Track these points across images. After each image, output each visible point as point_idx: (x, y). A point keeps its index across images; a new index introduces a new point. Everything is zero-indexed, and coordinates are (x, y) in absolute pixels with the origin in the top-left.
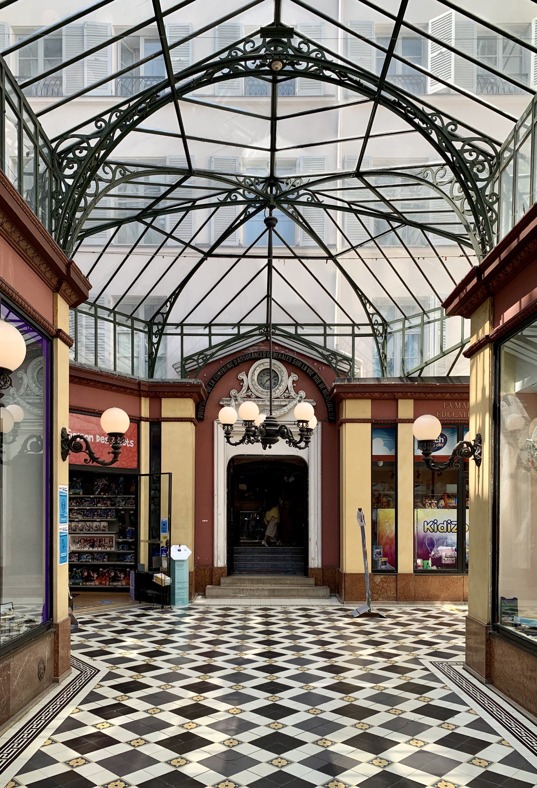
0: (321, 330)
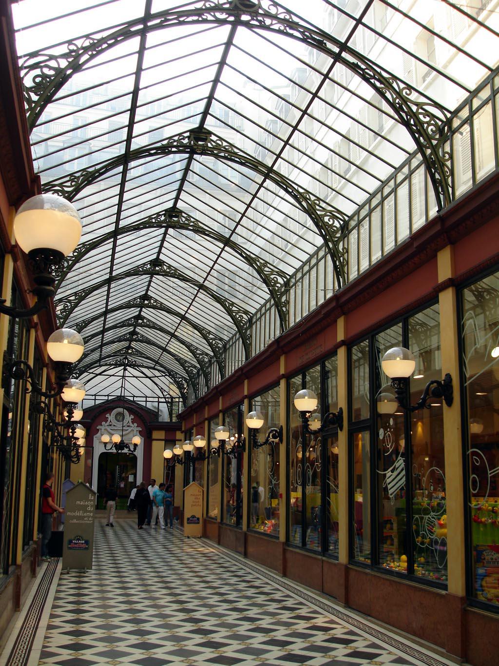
0: (144, 399)
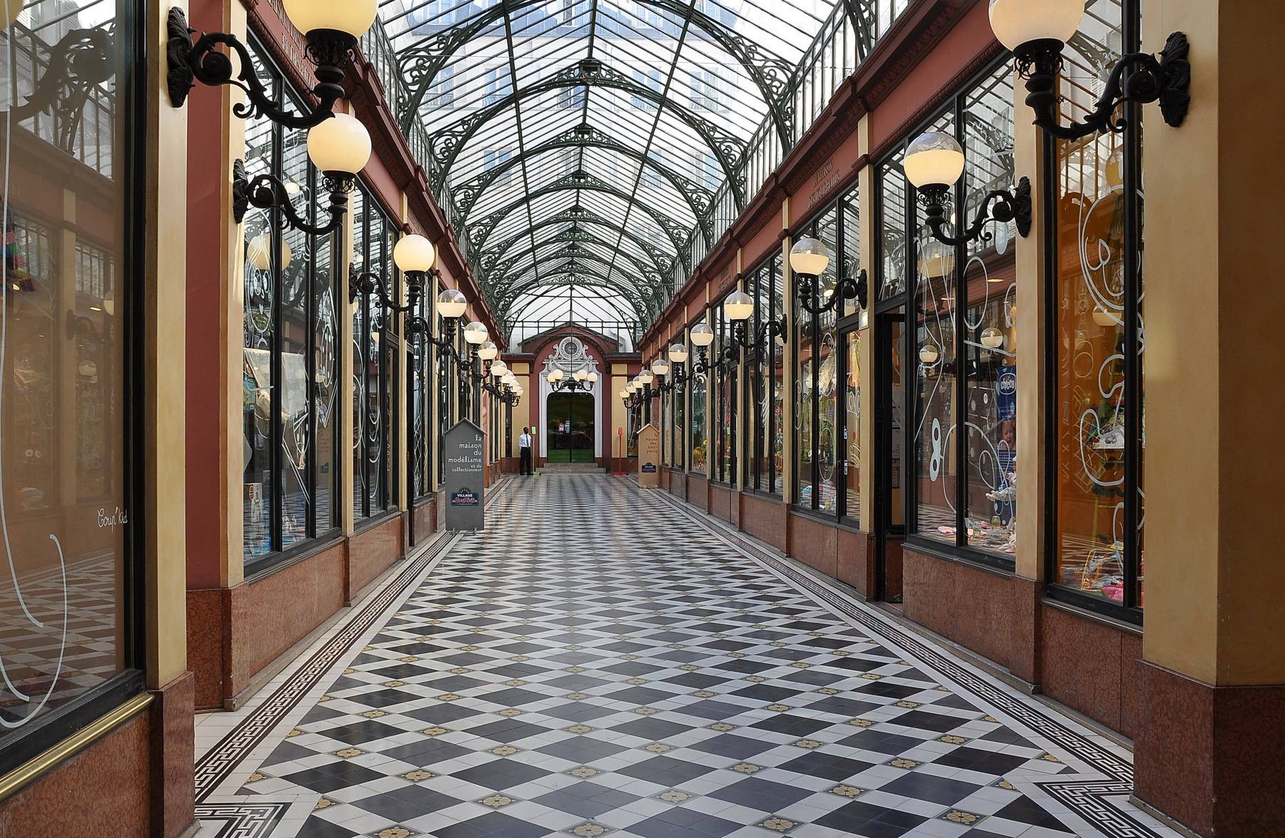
0: (600, 325)
